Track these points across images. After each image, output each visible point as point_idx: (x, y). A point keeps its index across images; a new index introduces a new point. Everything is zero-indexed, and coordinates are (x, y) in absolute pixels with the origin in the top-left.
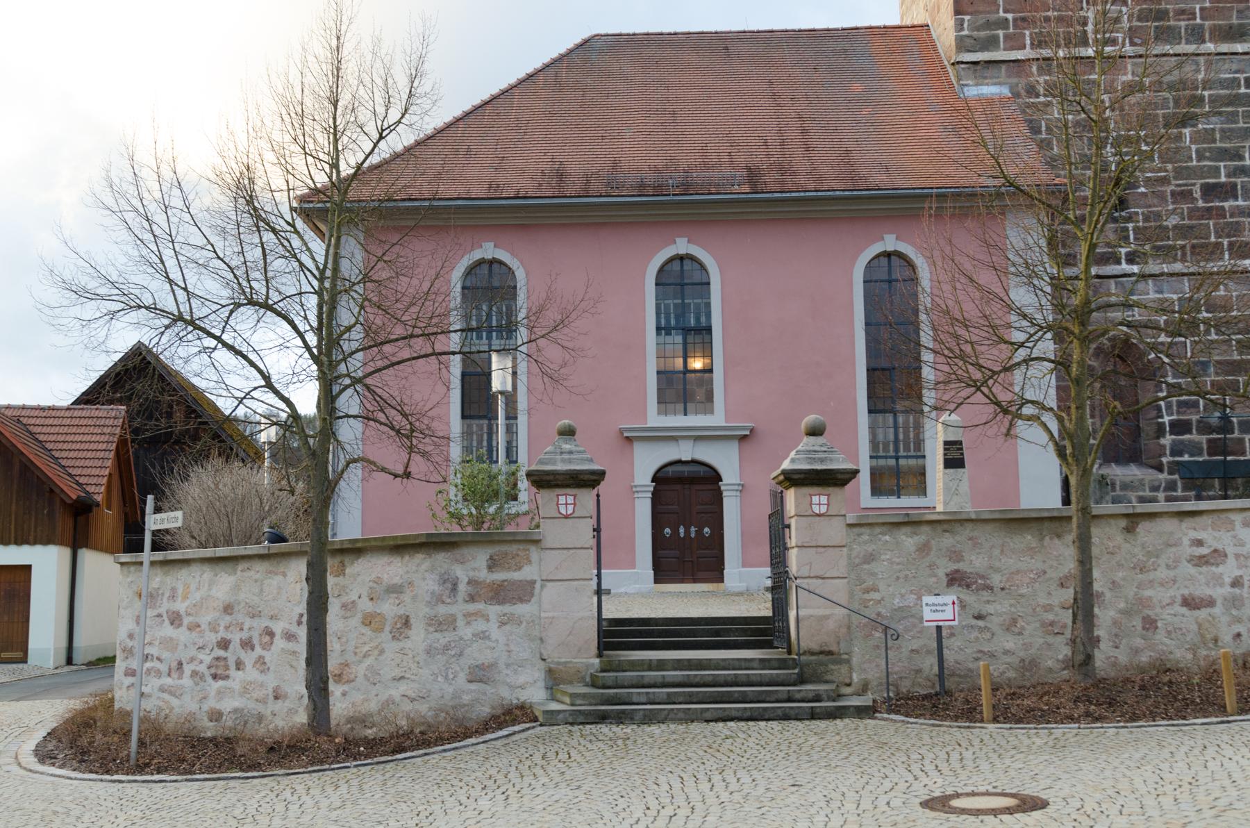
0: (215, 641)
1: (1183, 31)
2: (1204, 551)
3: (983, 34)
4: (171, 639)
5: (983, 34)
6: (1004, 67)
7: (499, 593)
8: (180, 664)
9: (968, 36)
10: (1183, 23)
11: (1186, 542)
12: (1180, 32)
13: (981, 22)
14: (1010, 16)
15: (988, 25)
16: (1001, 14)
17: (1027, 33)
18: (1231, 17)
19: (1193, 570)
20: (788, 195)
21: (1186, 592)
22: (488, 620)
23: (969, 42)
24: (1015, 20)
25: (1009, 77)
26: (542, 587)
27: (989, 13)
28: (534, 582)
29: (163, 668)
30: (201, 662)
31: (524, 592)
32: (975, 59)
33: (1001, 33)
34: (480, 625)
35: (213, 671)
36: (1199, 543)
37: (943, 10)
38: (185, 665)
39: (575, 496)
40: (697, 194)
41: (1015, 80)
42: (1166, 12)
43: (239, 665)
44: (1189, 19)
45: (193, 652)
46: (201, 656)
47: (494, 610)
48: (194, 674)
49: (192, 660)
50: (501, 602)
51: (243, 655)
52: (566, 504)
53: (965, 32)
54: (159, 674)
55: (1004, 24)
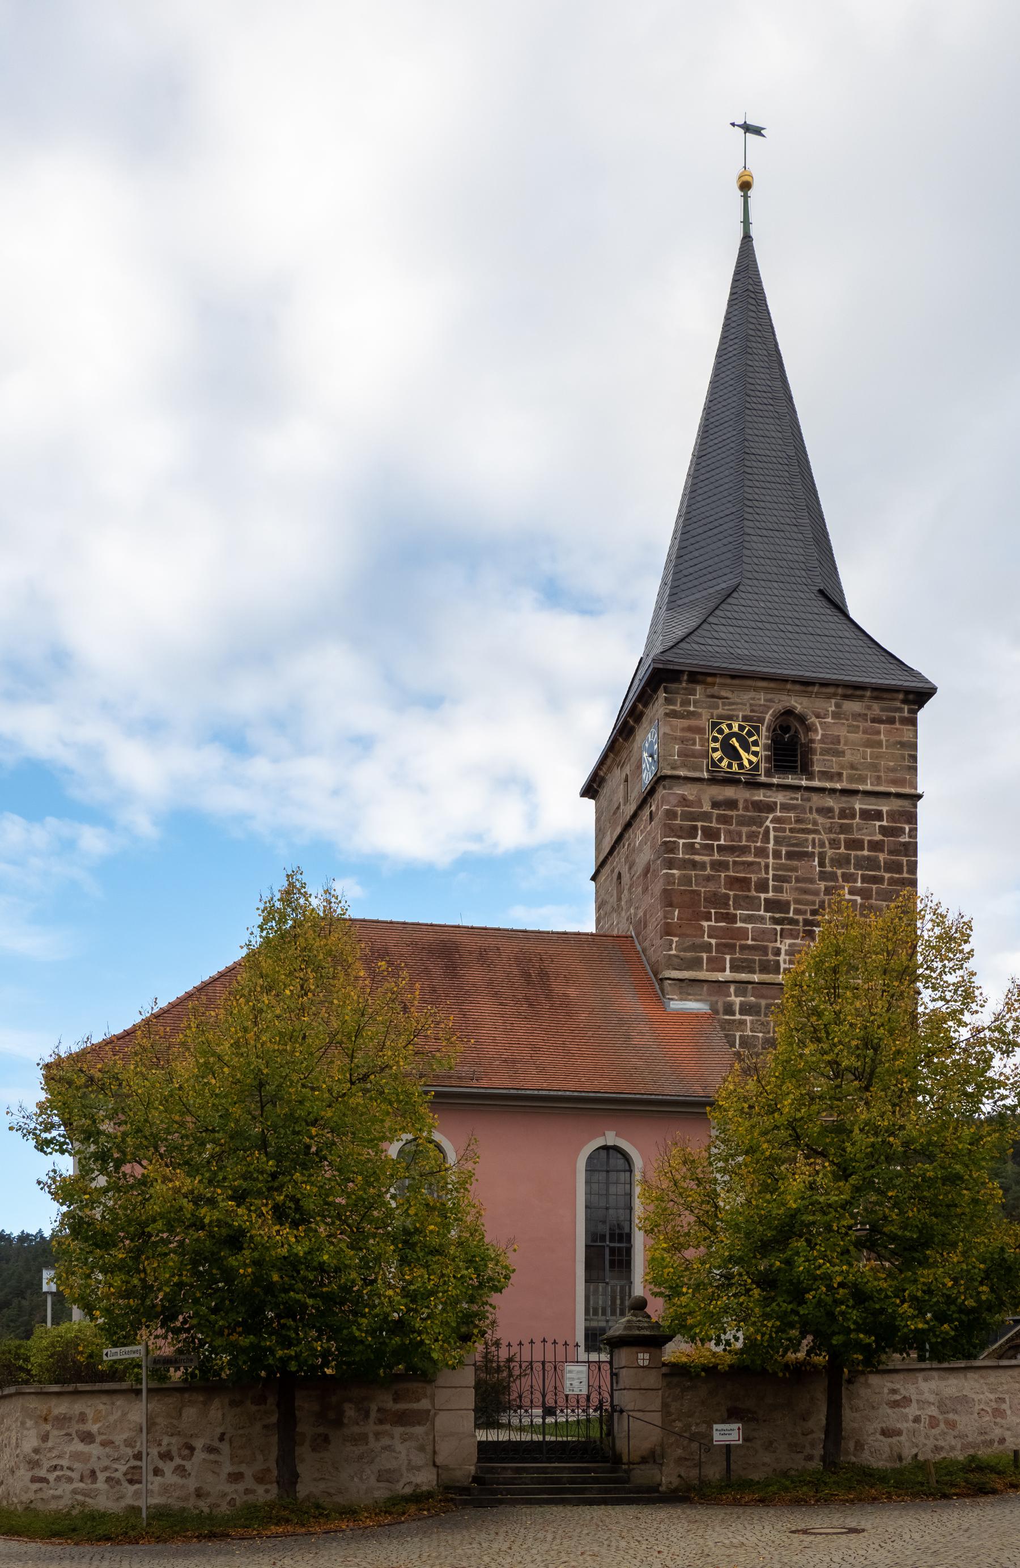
0: (131, 1454)
2: (898, 1397)
4: (82, 1453)
6: (705, 987)
7: (402, 1419)
8: (93, 1473)
9: (674, 955)
11: (886, 1391)
14: (713, 941)
15: (694, 948)
16: (706, 938)
17: (728, 957)
19: (889, 1411)
21: (884, 1425)
22: (393, 1438)
23: (676, 961)
24: (717, 945)
25: (710, 995)
26: (435, 1414)
27: (695, 936)
28: (429, 1411)
29: (75, 1475)
30: (116, 1470)
31: (423, 1417)
32: (680, 977)
33: (705, 955)
34: (385, 1441)
35: (129, 1477)
36: (894, 1391)
37: (650, 927)
38: (98, 1473)
41: (714, 999)
43: (157, 1472)
45: (106, 1462)
46: (116, 1466)
47: (398, 1430)
48: (108, 1480)
49: (106, 1469)
50: (402, 1426)
51: (161, 1464)
53: (673, 952)
54: (70, 1480)
55: (707, 948)
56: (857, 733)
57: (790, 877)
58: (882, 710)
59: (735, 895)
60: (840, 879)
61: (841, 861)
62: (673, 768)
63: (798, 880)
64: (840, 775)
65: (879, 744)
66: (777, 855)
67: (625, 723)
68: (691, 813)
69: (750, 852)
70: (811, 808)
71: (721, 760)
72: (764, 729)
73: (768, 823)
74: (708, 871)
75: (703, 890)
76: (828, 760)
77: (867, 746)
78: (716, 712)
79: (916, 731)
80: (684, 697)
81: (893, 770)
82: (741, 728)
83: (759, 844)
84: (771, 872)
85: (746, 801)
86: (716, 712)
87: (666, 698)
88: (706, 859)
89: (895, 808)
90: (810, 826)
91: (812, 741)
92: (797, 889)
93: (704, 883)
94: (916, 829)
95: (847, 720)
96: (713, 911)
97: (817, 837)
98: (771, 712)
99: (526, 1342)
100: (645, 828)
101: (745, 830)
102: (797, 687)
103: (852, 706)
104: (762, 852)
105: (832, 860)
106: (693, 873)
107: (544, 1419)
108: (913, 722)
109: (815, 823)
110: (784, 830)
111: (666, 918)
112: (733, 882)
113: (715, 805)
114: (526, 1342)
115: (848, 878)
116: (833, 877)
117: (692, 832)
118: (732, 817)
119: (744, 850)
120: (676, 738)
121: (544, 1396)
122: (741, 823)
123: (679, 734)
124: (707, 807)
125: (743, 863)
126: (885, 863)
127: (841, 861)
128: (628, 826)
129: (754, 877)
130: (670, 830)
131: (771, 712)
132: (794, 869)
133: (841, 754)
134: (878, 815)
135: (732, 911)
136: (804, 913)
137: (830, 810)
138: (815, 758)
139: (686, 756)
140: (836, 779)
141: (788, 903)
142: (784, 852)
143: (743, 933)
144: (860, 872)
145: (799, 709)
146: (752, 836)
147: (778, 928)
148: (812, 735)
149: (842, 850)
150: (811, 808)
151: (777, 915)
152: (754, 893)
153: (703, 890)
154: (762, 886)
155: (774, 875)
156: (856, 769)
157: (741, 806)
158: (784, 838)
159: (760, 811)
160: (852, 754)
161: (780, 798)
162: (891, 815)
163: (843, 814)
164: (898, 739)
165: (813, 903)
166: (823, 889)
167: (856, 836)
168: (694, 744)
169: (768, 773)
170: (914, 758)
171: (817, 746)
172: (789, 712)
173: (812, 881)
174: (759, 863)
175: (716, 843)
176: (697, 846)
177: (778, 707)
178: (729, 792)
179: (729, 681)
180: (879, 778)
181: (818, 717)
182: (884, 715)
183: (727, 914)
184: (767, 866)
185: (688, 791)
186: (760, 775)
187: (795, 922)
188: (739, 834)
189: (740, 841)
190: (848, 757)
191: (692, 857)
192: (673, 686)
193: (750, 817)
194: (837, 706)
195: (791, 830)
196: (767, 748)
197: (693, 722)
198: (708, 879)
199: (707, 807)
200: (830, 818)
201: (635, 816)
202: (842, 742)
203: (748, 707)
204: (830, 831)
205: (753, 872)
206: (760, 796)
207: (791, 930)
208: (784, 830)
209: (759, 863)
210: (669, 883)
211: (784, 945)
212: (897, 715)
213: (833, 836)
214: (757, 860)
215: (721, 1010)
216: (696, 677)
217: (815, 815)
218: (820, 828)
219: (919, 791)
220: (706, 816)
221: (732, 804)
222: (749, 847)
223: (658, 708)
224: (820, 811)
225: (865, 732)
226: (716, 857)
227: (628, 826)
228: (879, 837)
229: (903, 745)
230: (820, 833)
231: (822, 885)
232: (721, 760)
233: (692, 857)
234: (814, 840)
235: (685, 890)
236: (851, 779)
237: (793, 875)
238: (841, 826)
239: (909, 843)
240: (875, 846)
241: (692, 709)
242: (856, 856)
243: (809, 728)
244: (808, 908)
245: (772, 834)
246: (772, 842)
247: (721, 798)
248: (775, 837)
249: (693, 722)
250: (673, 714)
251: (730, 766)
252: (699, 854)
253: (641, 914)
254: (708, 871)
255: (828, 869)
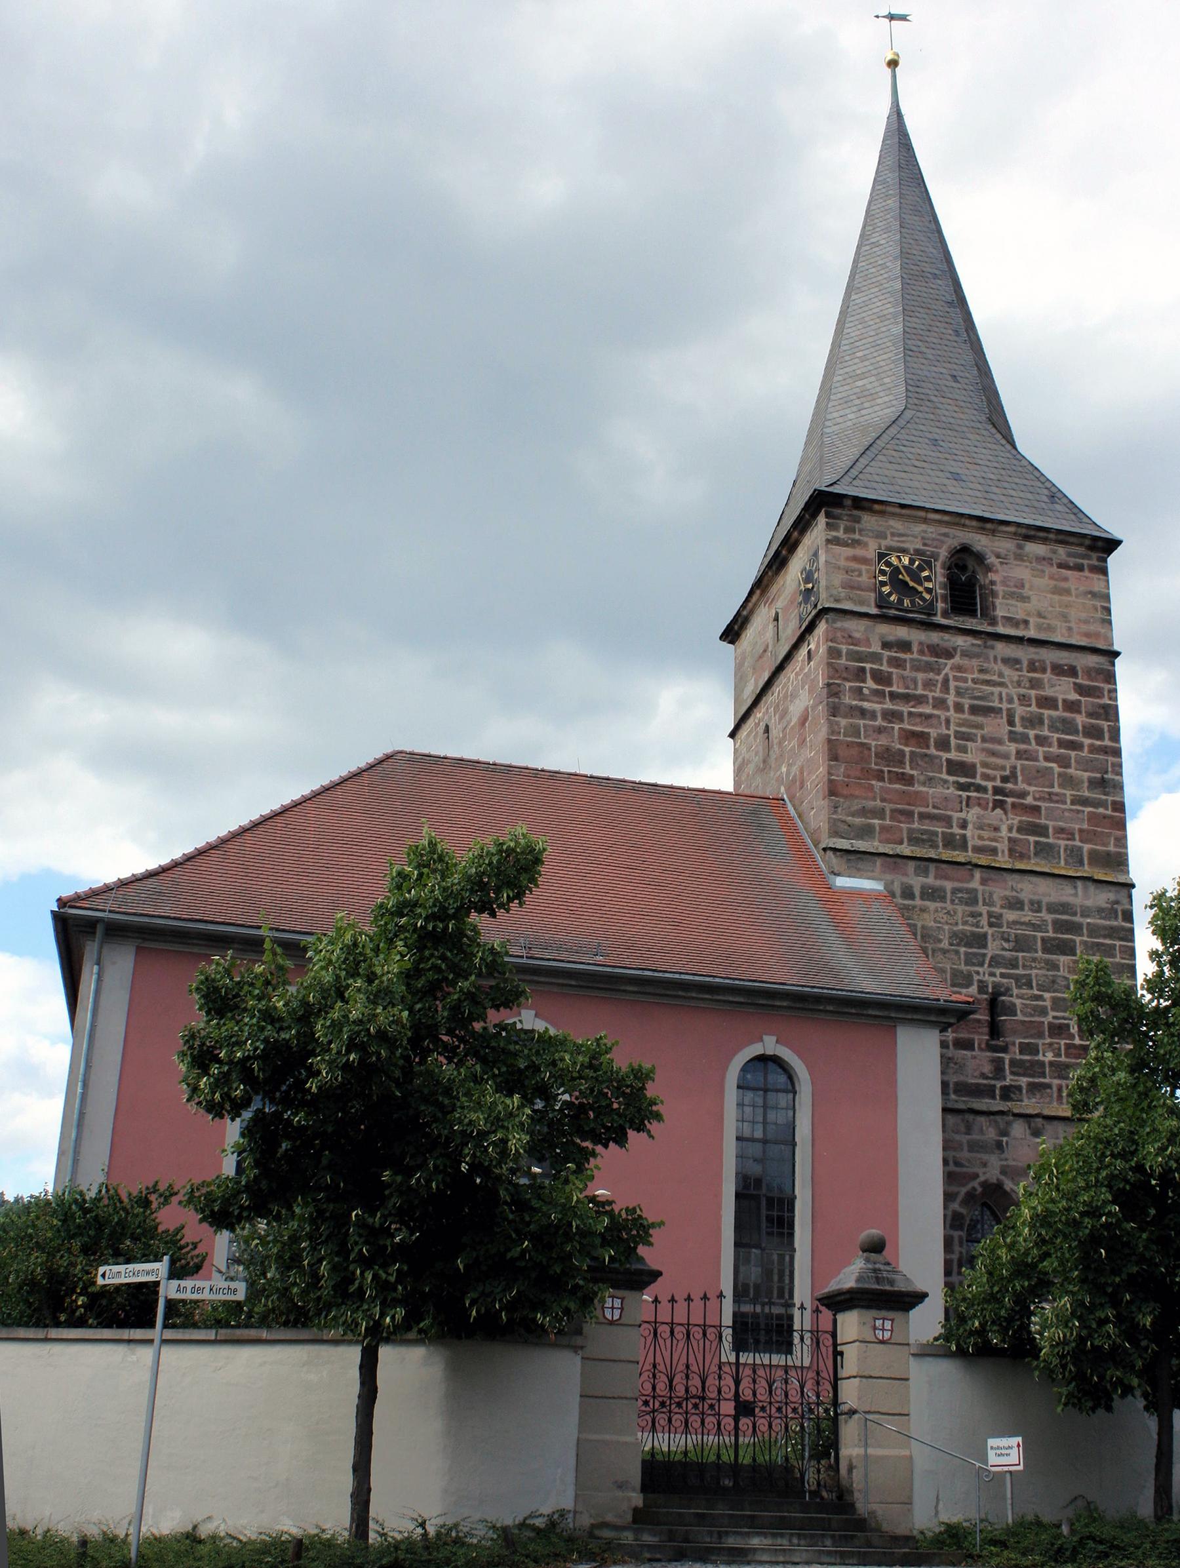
1: (1062, 851)
3: (858, 821)
5: (858, 821)
10: (1062, 843)
12: (1059, 853)
13: (856, 808)
18: (1109, 843)
20: (660, 975)
24: (893, 811)
25: (884, 872)
27: (865, 798)
39: (623, 1299)
40: (554, 960)
41: (889, 877)
42: (1046, 828)
44: (1068, 839)
52: (613, 1308)
56: (1042, 577)
57: (975, 735)
58: (1069, 555)
59: (912, 753)
60: (1033, 742)
61: (1033, 721)
62: (837, 601)
63: (984, 740)
64: (1026, 622)
65: (1067, 592)
66: (959, 708)
67: (777, 553)
68: (857, 652)
69: (928, 703)
70: (995, 658)
71: (890, 594)
72: (939, 564)
73: (947, 670)
74: (879, 722)
75: (874, 743)
76: (1012, 605)
77: (1053, 593)
78: (884, 543)
79: (1108, 581)
80: (848, 524)
81: (1086, 622)
82: (912, 561)
83: (938, 694)
84: (952, 727)
85: (921, 643)
86: (884, 543)
87: (827, 524)
88: (877, 707)
89: (1091, 665)
90: (995, 678)
91: (992, 583)
92: (983, 750)
93: (875, 735)
94: (1115, 690)
95: (1031, 563)
96: (886, 769)
97: (1004, 691)
98: (945, 547)
99: (696, 1296)
100: (802, 669)
101: (921, 676)
102: (974, 523)
103: (1034, 549)
104: (940, 703)
105: (1022, 718)
106: (862, 722)
107: (737, 1421)
108: (1104, 571)
109: (1001, 675)
110: (965, 680)
111: (830, 774)
112: (911, 737)
113: (886, 645)
114: (696, 1296)
115: (1041, 741)
116: (1024, 739)
117: (860, 674)
118: (905, 661)
119: (920, 700)
120: (839, 568)
121: (737, 1382)
122: (917, 669)
123: (842, 563)
124: (876, 648)
125: (920, 715)
126: (1084, 727)
127: (1033, 721)
128: (780, 668)
129: (933, 733)
130: (833, 669)
131: (945, 547)
132: (980, 726)
133: (1025, 599)
134: (1072, 672)
135: (908, 770)
136: (993, 779)
137: (1017, 661)
138: (998, 602)
139: (852, 588)
140: (1022, 626)
141: (974, 766)
142: (966, 706)
143: (921, 799)
144: (1056, 736)
145: (977, 547)
146: (929, 684)
147: (964, 794)
148: (991, 576)
149: (1034, 708)
150: (995, 658)
151: (962, 780)
152: (933, 751)
153: (874, 743)
154: (943, 744)
155: (956, 732)
156: (1044, 618)
157: (915, 648)
158: (967, 689)
159: (937, 655)
160: (1039, 601)
161: (961, 641)
162: (1090, 672)
163: (1032, 667)
164: (1089, 589)
165: (1003, 768)
166: (1014, 752)
167: (1049, 692)
168: (860, 575)
169: (945, 614)
170: (1108, 610)
171: (999, 588)
172: (965, 550)
173: (999, 742)
174: (939, 717)
175: (888, 689)
176: (866, 691)
177: (955, 543)
178: (901, 632)
179: (898, 510)
180: (1070, 629)
181: (998, 557)
182: (1072, 561)
183: (903, 774)
184: (948, 721)
185: (857, 627)
186: (935, 615)
187: (983, 789)
188: (915, 681)
189: (916, 689)
190: (1035, 603)
191: (860, 703)
192: (837, 511)
193: (927, 662)
194: (1020, 547)
195: (974, 681)
196: (944, 587)
197: (859, 552)
198: (880, 730)
199: (876, 648)
200: (1017, 670)
201: (788, 657)
202: (1027, 586)
203: (919, 539)
204: (1019, 685)
205: (931, 726)
206: (935, 637)
207: (979, 798)
208: (965, 680)
209: (939, 717)
210: (833, 733)
211: (972, 814)
212: (1085, 562)
213: (1022, 691)
214: (936, 712)
215: (898, 892)
216: (860, 504)
217: (1000, 666)
218: (1006, 680)
219: (1116, 648)
220: (875, 658)
221: (905, 646)
222: (926, 696)
223: (818, 532)
224: (1006, 661)
225: (1051, 578)
226: (889, 705)
227: (780, 668)
228: (1074, 696)
229: (1094, 595)
230: (1007, 687)
231: (1012, 748)
232: (890, 594)
233: (860, 703)
234: (1000, 694)
235: (852, 742)
236: (1039, 627)
237: (979, 733)
238: (1031, 680)
239: (1109, 705)
240: (1072, 706)
241: (857, 536)
242: (1050, 718)
243: (989, 569)
244: (998, 774)
245: (952, 684)
246: (952, 691)
247: (891, 638)
248: (957, 688)
249: (859, 552)
250: (835, 541)
251: (900, 601)
252: (868, 701)
253: (795, 769)
254: (879, 722)
255: (1019, 729)
